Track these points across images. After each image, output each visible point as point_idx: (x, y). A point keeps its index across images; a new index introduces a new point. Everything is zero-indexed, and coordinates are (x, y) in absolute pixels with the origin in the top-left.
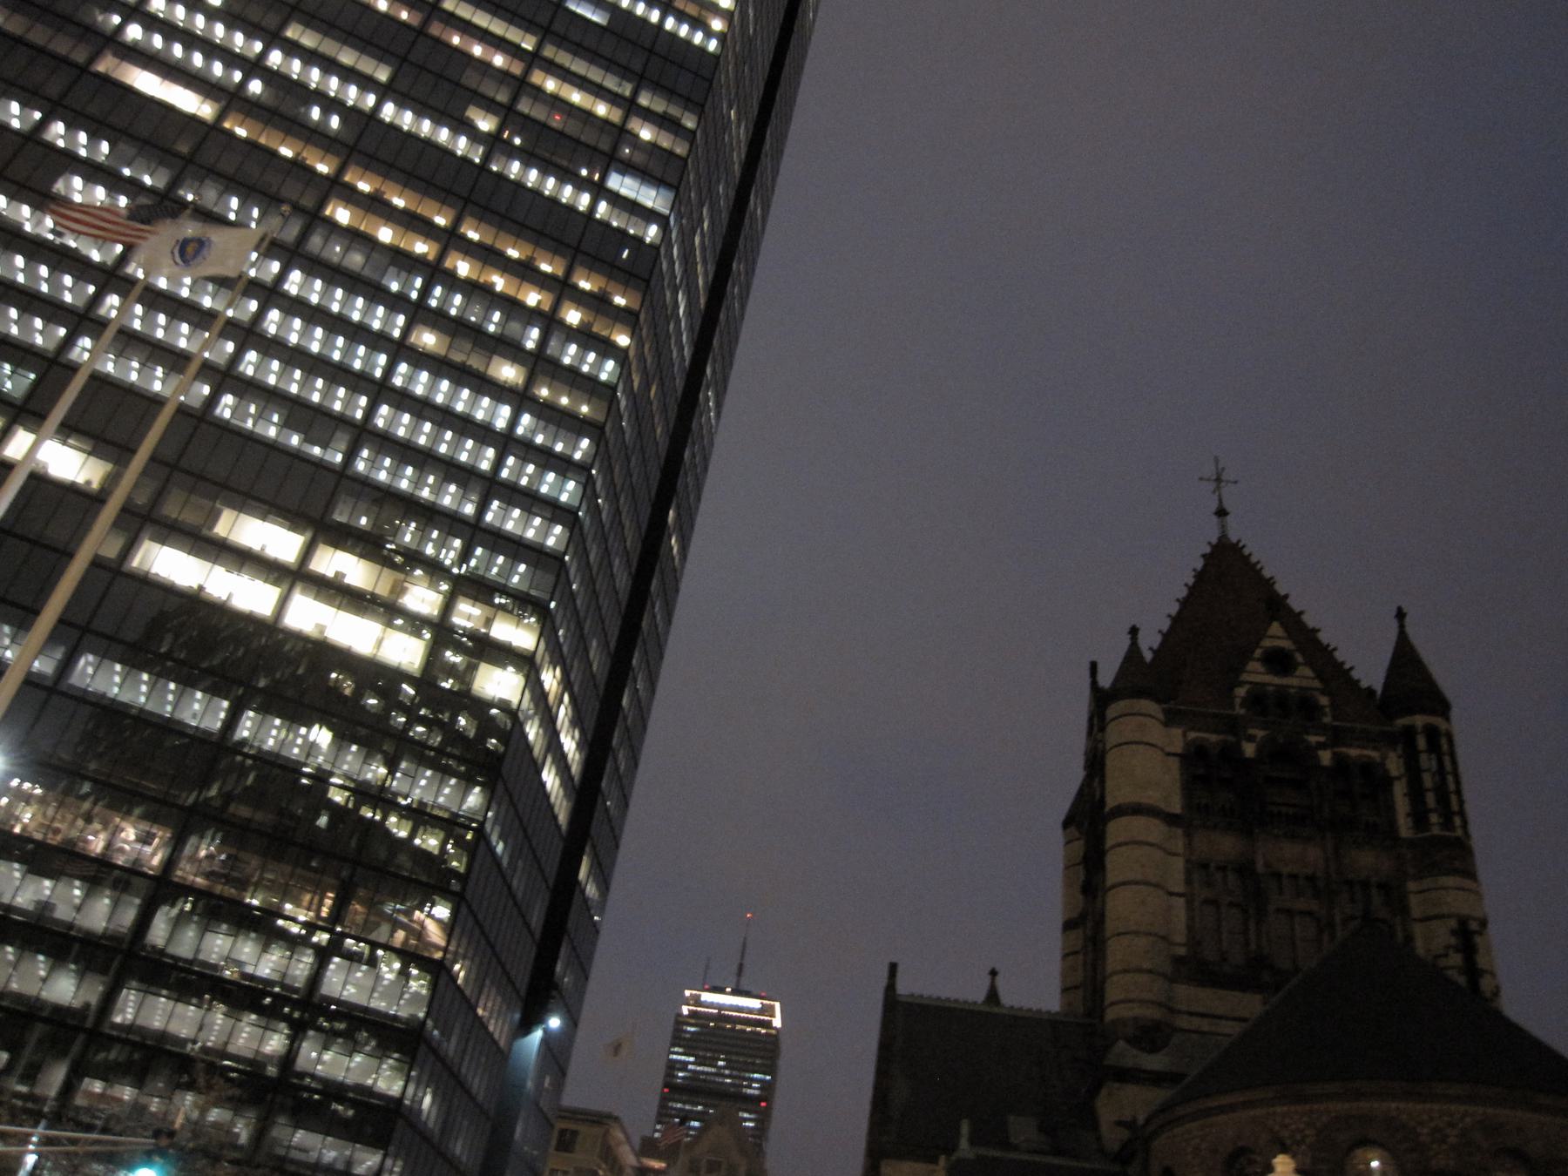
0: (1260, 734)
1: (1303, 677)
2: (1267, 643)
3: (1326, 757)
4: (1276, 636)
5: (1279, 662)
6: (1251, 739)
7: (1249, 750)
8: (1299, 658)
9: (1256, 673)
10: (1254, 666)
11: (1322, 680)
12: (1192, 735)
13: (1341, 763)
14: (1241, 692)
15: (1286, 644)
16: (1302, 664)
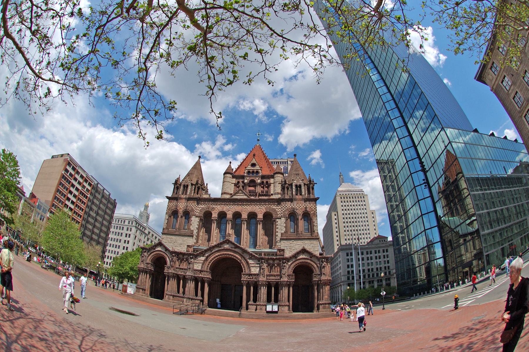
0: (248, 178)
1: (257, 167)
2: (252, 162)
3: (259, 181)
4: (254, 161)
5: (253, 165)
7: (246, 181)
9: (249, 167)
13: (263, 182)
14: (246, 171)
15: (256, 162)
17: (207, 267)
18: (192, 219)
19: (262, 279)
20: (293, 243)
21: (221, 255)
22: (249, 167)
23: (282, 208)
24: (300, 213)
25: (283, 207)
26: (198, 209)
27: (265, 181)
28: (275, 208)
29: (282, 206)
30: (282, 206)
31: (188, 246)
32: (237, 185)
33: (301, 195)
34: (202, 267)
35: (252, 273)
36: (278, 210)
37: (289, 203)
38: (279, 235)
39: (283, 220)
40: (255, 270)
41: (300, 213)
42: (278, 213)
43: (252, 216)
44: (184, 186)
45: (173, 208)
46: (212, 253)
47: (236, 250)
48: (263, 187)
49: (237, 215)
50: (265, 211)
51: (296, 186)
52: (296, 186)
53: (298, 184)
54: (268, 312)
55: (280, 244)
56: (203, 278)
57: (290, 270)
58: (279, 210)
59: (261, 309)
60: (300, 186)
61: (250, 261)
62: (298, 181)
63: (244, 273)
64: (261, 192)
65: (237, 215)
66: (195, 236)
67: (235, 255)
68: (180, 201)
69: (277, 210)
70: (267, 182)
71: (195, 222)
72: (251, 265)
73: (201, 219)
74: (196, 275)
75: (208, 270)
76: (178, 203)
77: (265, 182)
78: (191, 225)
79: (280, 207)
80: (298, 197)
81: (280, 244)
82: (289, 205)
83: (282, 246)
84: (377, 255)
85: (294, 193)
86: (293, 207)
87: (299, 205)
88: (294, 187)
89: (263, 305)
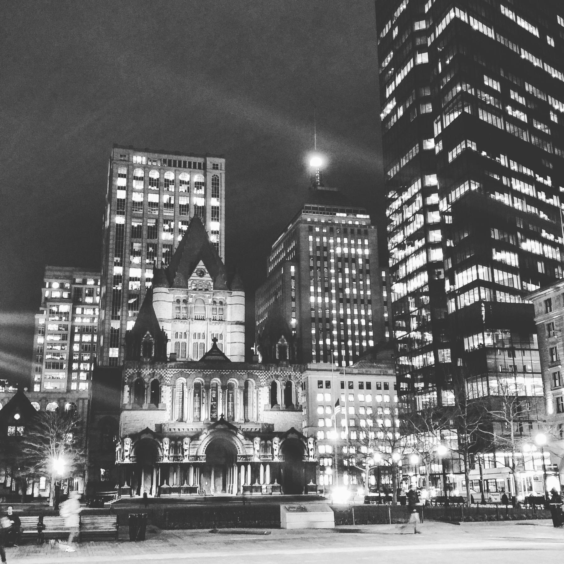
6: (192, 297)
18: (163, 389)
25: (266, 373)
28: (258, 374)
29: (265, 373)
30: (265, 373)
36: (261, 378)
42: (261, 381)
51: (280, 347)
52: (280, 347)
63: (239, 454)
69: (259, 377)
75: (204, 455)
78: (163, 397)
79: (262, 373)
83: (265, 419)
86: (277, 374)
87: (283, 372)
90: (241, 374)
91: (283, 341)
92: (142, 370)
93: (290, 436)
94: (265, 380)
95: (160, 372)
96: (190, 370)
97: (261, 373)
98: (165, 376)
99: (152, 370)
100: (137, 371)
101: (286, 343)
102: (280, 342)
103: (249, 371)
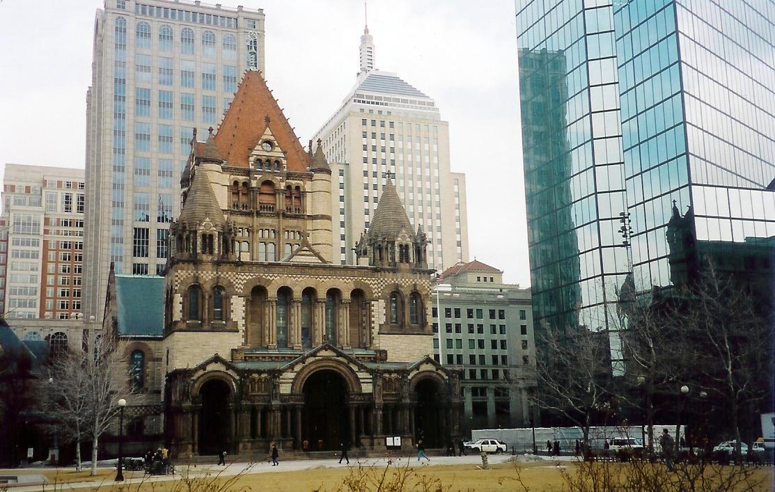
0: (259, 176)
1: (277, 153)
2: (264, 137)
3: (283, 186)
4: (268, 135)
7: (254, 184)
8: (277, 144)
10: (258, 147)
11: (285, 153)
12: (232, 177)
13: (289, 187)
14: (252, 159)
15: (272, 138)
16: (277, 146)
17: (298, 389)
19: (379, 401)
20: (398, 340)
21: (319, 367)
22: (260, 151)
23: (379, 283)
24: (406, 291)
26: (241, 280)
27: (294, 182)
30: (379, 281)
31: (233, 350)
32: (235, 188)
33: (408, 261)
34: (292, 389)
35: (363, 392)
36: (374, 287)
37: (391, 274)
38: (377, 328)
39: (382, 303)
40: (367, 388)
41: (406, 291)
43: (334, 293)
44: (204, 236)
45: (189, 281)
46: (306, 366)
47: (340, 358)
48: (289, 197)
49: (309, 292)
50: (352, 287)
51: (401, 246)
52: (401, 246)
53: (404, 243)
54: (389, 448)
55: (377, 341)
56: (294, 406)
57: (411, 387)
58: (376, 285)
59: (379, 444)
60: (407, 246)
61: (360, 375)
62: (403, 237)
64: (285, 209)
65: (309, 292)
66: (241, 331)
67: (338, 366)
68: (200, 267)
70: (298, 188)
71: (238, 308)
72: (361, 381)
73: (247, 301)
74: (285, 404)
76: (197, 270)
77: (293, 187)
80: (404, 266)
81: (377, 341)
82: (390, 279)
84: (472, 321)
85: (397, 259)
86: (397, 282)
88: (397, 249)
89: (382, 438)
90: (345, 282)
91: (403, 237)
92: (200, 272)
93: (424, 367)
94: (379, 290)
95: (227, 275)
96: (271, 275)
97: (373, 281)
98: (234, 283)
99: (215, 273)
100: (192, 274)
101: (409, 239)
102: (399, 239)
103: (356, 278)
